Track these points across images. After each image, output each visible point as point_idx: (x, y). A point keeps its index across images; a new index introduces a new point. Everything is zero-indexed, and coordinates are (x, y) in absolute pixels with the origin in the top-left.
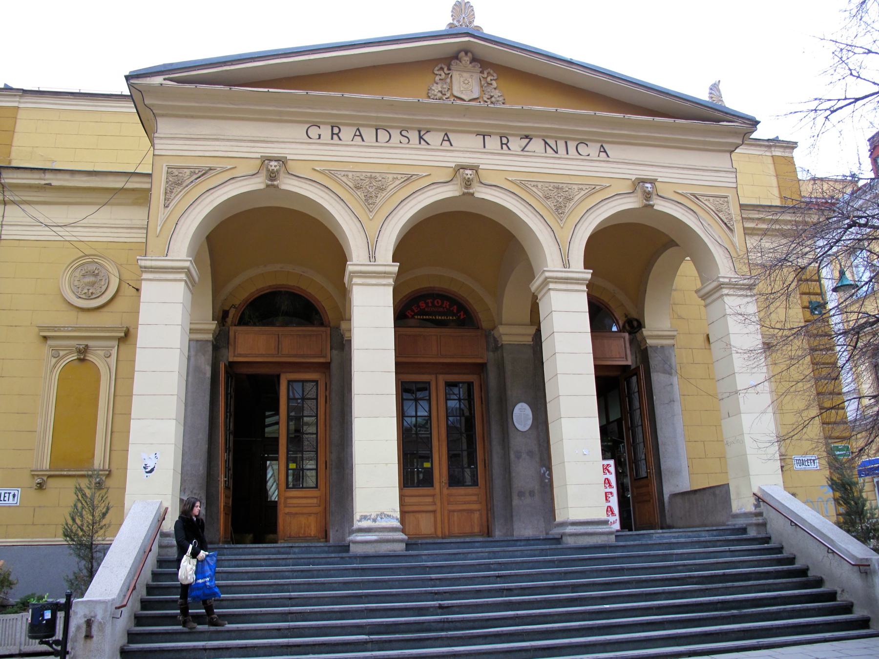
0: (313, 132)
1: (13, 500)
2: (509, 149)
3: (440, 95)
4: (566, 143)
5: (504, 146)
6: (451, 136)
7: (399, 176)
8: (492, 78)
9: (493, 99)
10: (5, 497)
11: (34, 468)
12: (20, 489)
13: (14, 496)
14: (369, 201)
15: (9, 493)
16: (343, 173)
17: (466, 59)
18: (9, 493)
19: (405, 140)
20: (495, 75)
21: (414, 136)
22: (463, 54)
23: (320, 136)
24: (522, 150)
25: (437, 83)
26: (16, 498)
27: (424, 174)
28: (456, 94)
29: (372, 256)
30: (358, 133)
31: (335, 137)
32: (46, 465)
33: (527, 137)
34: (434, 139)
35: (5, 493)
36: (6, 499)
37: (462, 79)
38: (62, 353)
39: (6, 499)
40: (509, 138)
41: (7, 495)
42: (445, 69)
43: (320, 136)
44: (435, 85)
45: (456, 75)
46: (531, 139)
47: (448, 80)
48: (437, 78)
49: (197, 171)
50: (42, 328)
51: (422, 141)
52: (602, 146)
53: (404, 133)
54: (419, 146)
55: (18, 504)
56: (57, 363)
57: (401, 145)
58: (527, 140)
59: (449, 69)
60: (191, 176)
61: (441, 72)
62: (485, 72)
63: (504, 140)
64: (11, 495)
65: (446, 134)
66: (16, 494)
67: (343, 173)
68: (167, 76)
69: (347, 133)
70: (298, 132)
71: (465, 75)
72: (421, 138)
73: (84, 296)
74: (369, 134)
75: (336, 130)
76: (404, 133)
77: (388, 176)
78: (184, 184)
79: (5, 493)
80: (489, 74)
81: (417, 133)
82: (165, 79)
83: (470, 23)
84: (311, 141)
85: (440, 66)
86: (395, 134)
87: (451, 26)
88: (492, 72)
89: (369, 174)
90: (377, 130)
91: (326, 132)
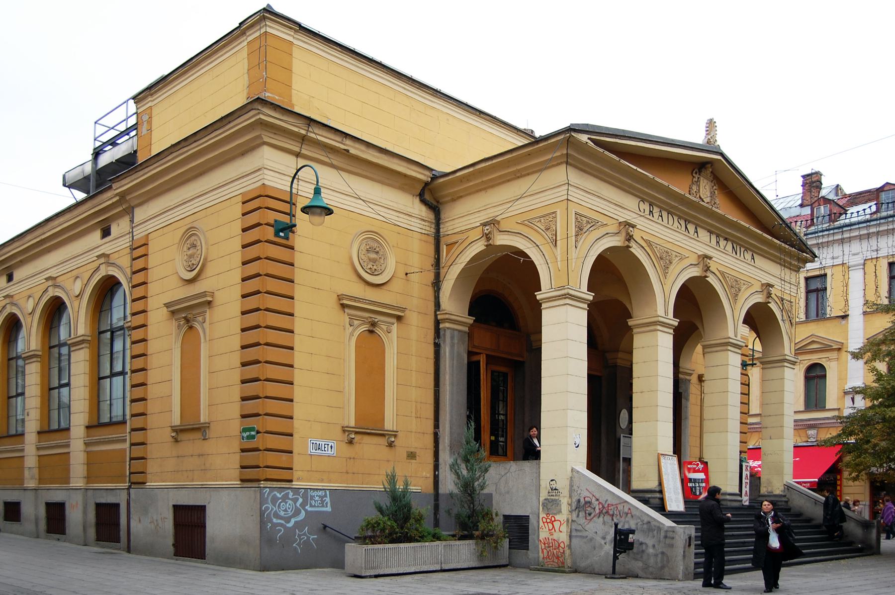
1: (331, 451)
10: (325, 447)
11: (346, 424)
12: (335, 442)
13: (331, 446)
15: (328, 445)
18: (328, 445)
26: (333, 449)
32: (353, 424)
35: (325, 444)
36: (326, 449)
38: (356, 322)
39: (326, 449)
41: (326, 446)
50: (340, 297)
55: (335, 455)
56: (354, 330)
64: (329, 446)
66: (333, 445)
73: (369, 272)
79: (325, 444)
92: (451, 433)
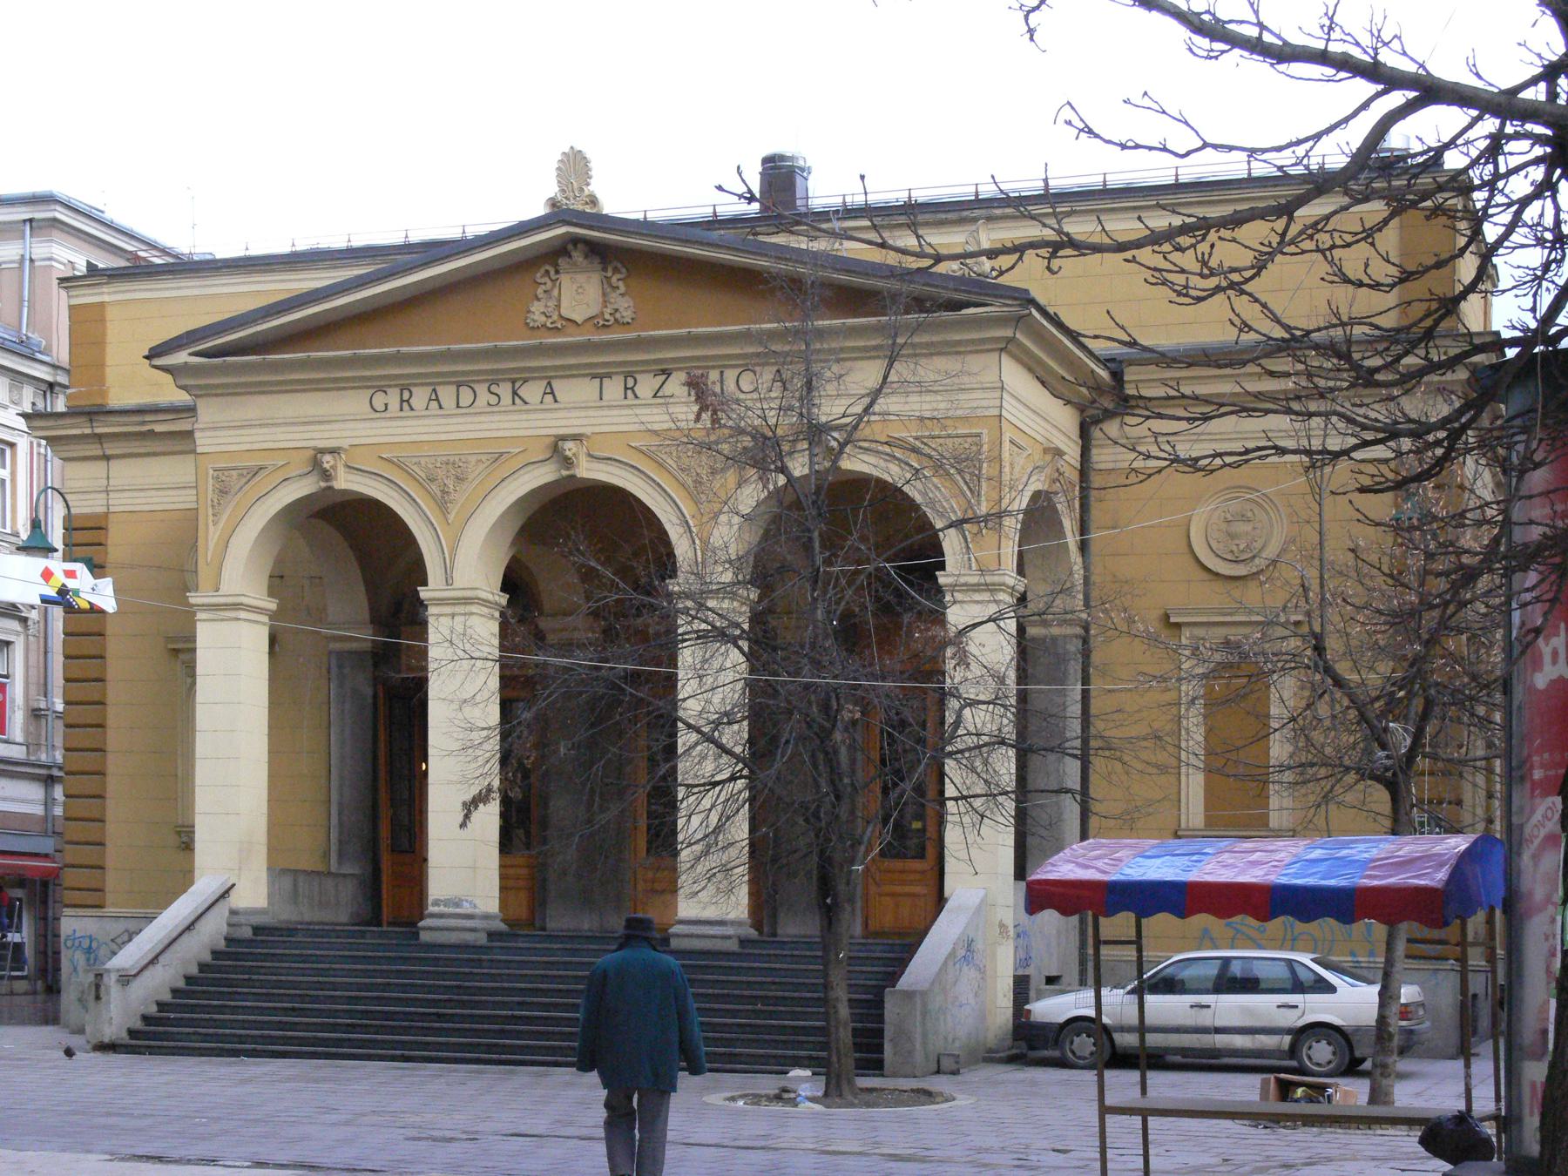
0: (379, 399)
2: (636, 397)
3: (543, 319)
4: (722, 372)
5: (629, 392)
6: (555, 384)
7: (484, 458)
8: (619, 276)
9: (618, 315)
14: (442, 502)
16: (414, 460)
17: (578, 256)
19: (494, 400)
20: (624, 270)
21: (505, 390)
22: (570, 247)
23: (386, 405)
24: (655, 396)
25: (538, 300)
27: (518, 450)
28: (564, 313)
29: (449, 580)
30: (434, 397)
31: (405, 405)
33: (663, 372)
34: (532, 392)
37: (575, 287)
40: (638, 376)
42: (552, 273)
43: (386, 405)
44: (536, 303)
45: (565, 279)
46: (669, 375)
47: (555, 293)
48: (540, 291)
49: (245, 472)
51: (517, 400)
52: (778, 371)
53: (494, 389)
54: (512, 408)
57: (490, 409)
58: (664, 377)
59: (557, 272)
60: (239, 480)
61: (546, 279)
62: (610, 269)
63: (630, 383)
65: (549, 383)
67: (414, 460)
68: (191, 350)
69: (420, 397)
70: (354, 403)
71: (581, 278)
72: (515, 393)
74: (447, 394)
75: (406, 395)
76: (494, 389)
77: (469, 458)
78: (233, 491)
80: (616, 270)
81: (509, 385)
82: (190, 354)
83: (582, 190)
84: (378, 415)
85: (542, 271)
86: (482, 389)
87: (553, 203)
88: (619, 265)
89: (445, 459)
90: (458, 386)
91: (393, 398)
92: (341, 824)
